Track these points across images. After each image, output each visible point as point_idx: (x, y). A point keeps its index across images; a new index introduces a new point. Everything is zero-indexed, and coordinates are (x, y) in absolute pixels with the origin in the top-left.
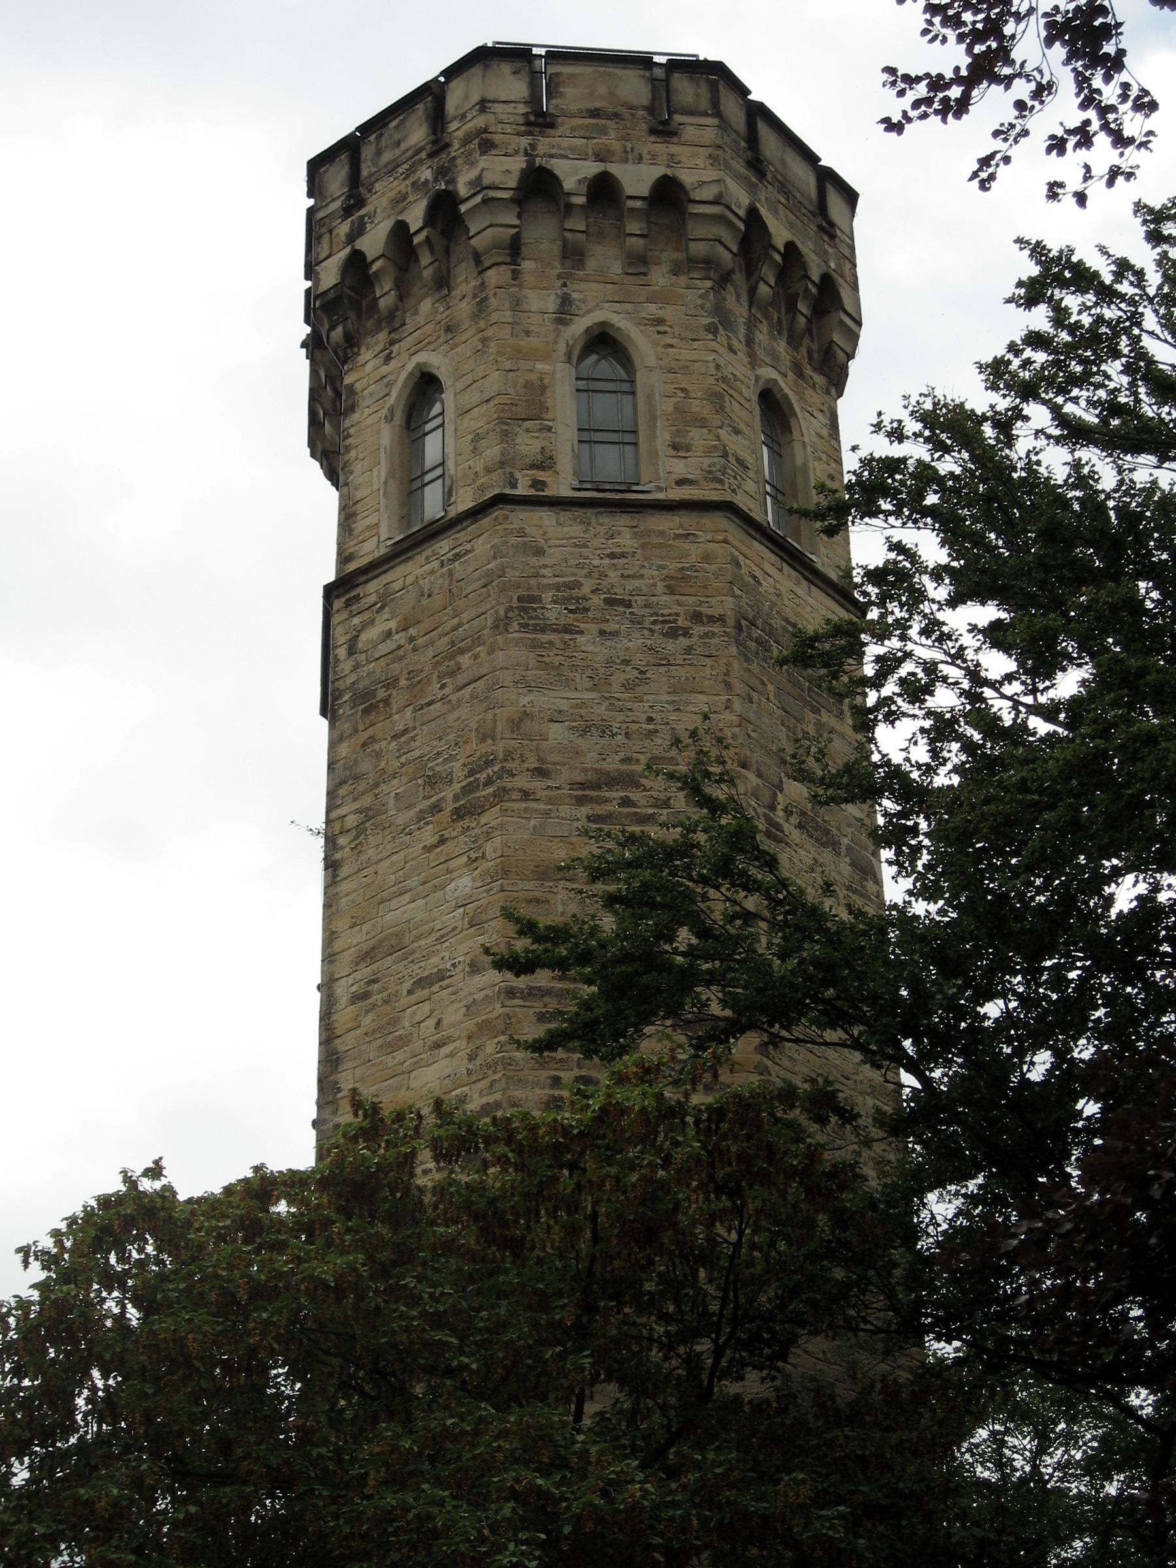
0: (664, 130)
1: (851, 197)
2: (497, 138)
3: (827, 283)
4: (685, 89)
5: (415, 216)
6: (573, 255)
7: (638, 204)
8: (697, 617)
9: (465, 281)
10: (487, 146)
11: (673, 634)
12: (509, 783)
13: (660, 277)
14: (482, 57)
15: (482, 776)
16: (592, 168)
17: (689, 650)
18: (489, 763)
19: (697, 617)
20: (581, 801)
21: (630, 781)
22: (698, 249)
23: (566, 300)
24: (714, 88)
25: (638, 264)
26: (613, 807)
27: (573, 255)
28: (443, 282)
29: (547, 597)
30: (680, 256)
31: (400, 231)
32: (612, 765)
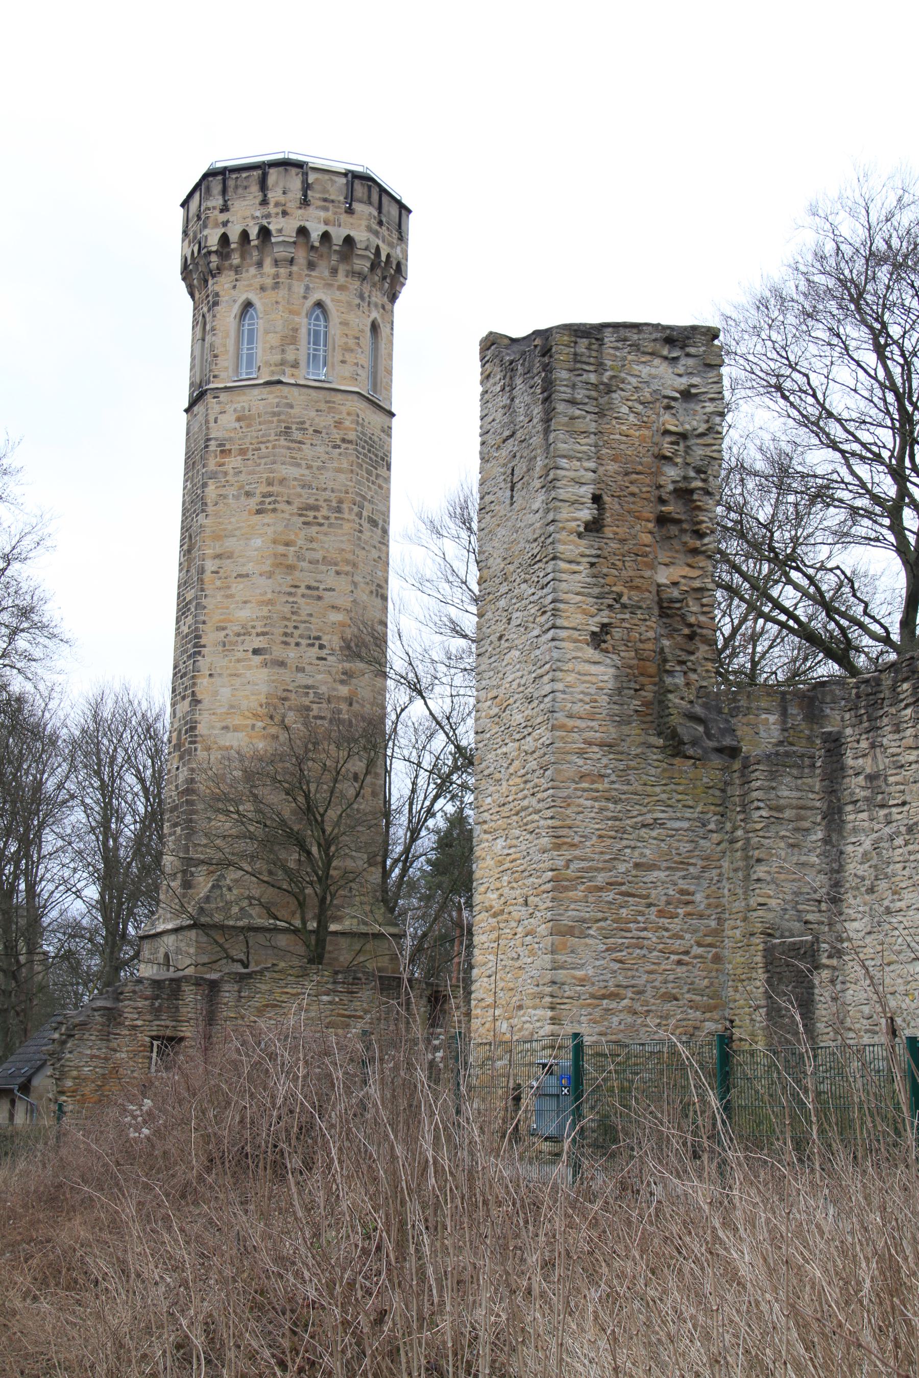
0: (350, 211)
1: (409, 211)
2: (289, 210)
3: (399, 265)
4: (360, 190)
5: (253, 232)
6: (311, 265)
7: (337, 248)
8: (343, 440)
9: (268, 268)
10: (285, 213)
11: (335, 447)
12: (277, 505)
13: (341, 278)
14: (285, 164)
15: (268, 500)
16: (323, 228)
17: (340, 454)
18: (270, 496)
19: (343, 440)
20: (301, 515)
21: (316, 508)
22: (357, 268)
23: (307, 288)
24: (369, 187)
25: (334, 271)
26: (310, 519)
27: (311, 265)
28: (260, 264)
29: (294, 427)
30: (348, 268)
31: (245, 235)
32: (311, 501)
